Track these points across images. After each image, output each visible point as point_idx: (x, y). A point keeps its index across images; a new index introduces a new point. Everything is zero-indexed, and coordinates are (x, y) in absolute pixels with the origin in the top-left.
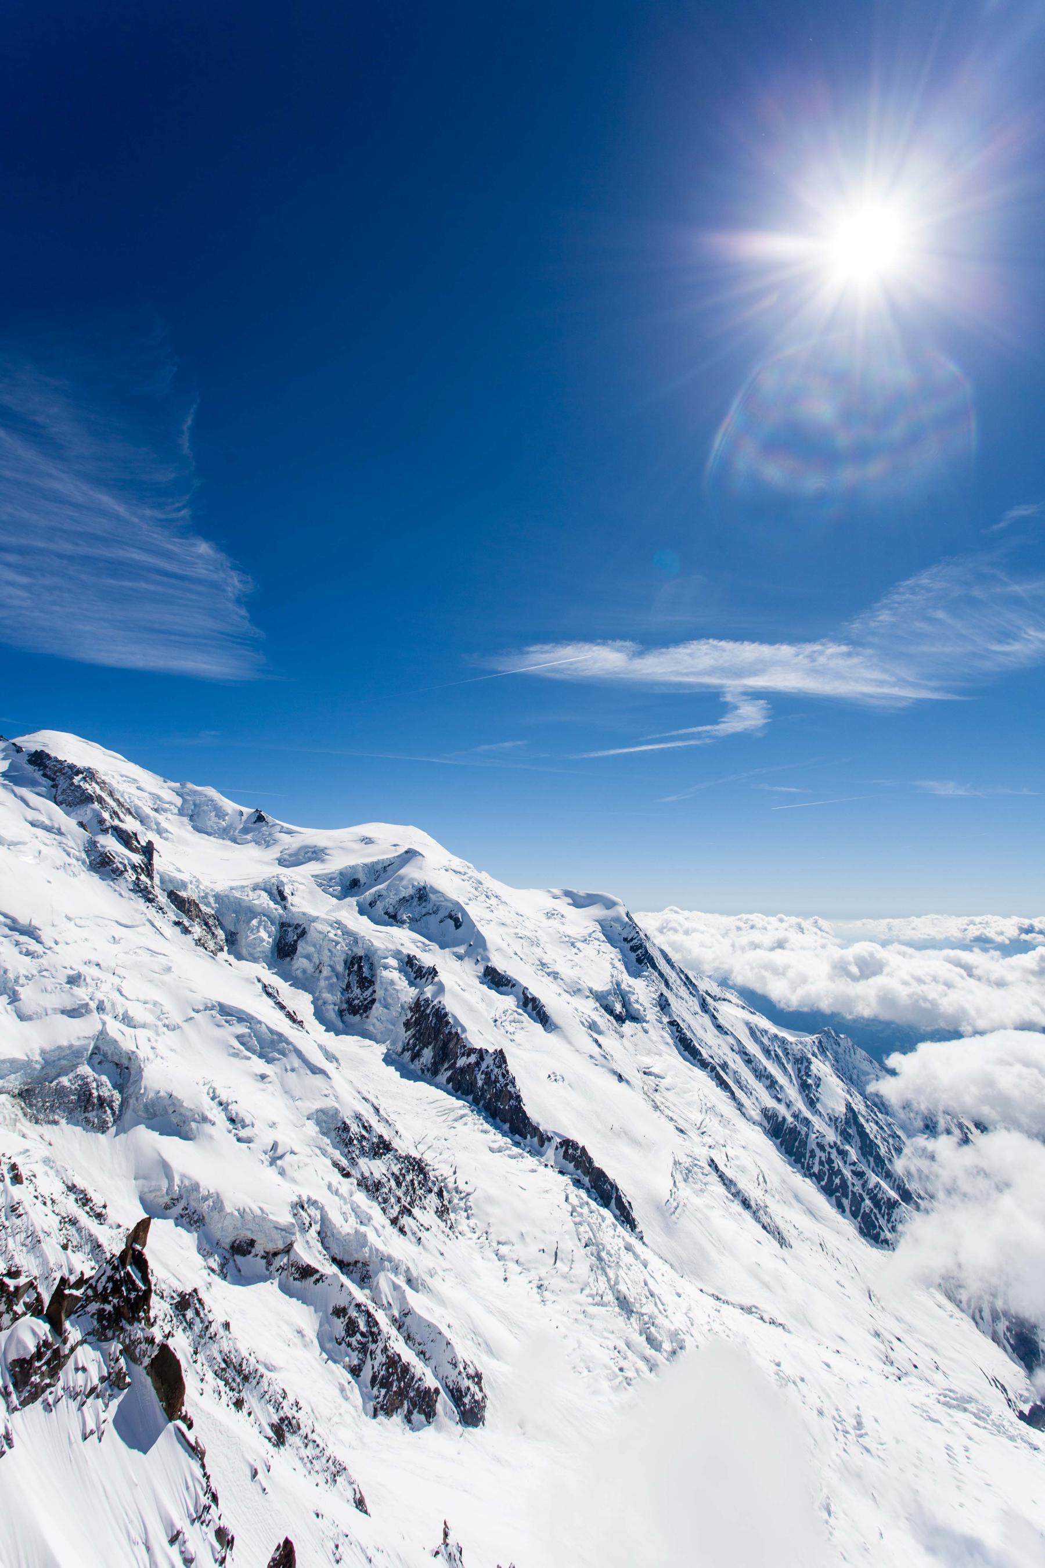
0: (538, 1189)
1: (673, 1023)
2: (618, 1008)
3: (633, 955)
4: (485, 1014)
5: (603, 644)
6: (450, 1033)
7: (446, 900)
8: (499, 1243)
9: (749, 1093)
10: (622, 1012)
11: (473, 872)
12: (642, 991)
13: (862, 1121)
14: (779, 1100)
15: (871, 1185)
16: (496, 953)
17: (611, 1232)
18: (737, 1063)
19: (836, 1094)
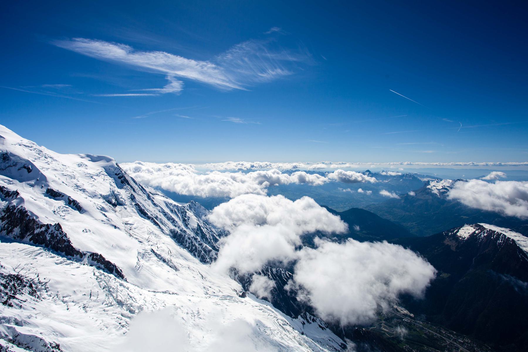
0: (84, 273)
1: (137, 205)
2: (114, 201)
3: (120, 180)
4: (49, 209)
5: (116, 44)
6: (29, 219)
7: (21, 159)
8: (63, 297)
9: (165, 225)
10: (114, 201)
11: (36, 146)
12: (123, 194)
13: (202, 228)
14: (176, 226)
15: (204, 247)
16: (52, 183)
17: (114, 281)
18: (161, 216)
19: (194, 221)
